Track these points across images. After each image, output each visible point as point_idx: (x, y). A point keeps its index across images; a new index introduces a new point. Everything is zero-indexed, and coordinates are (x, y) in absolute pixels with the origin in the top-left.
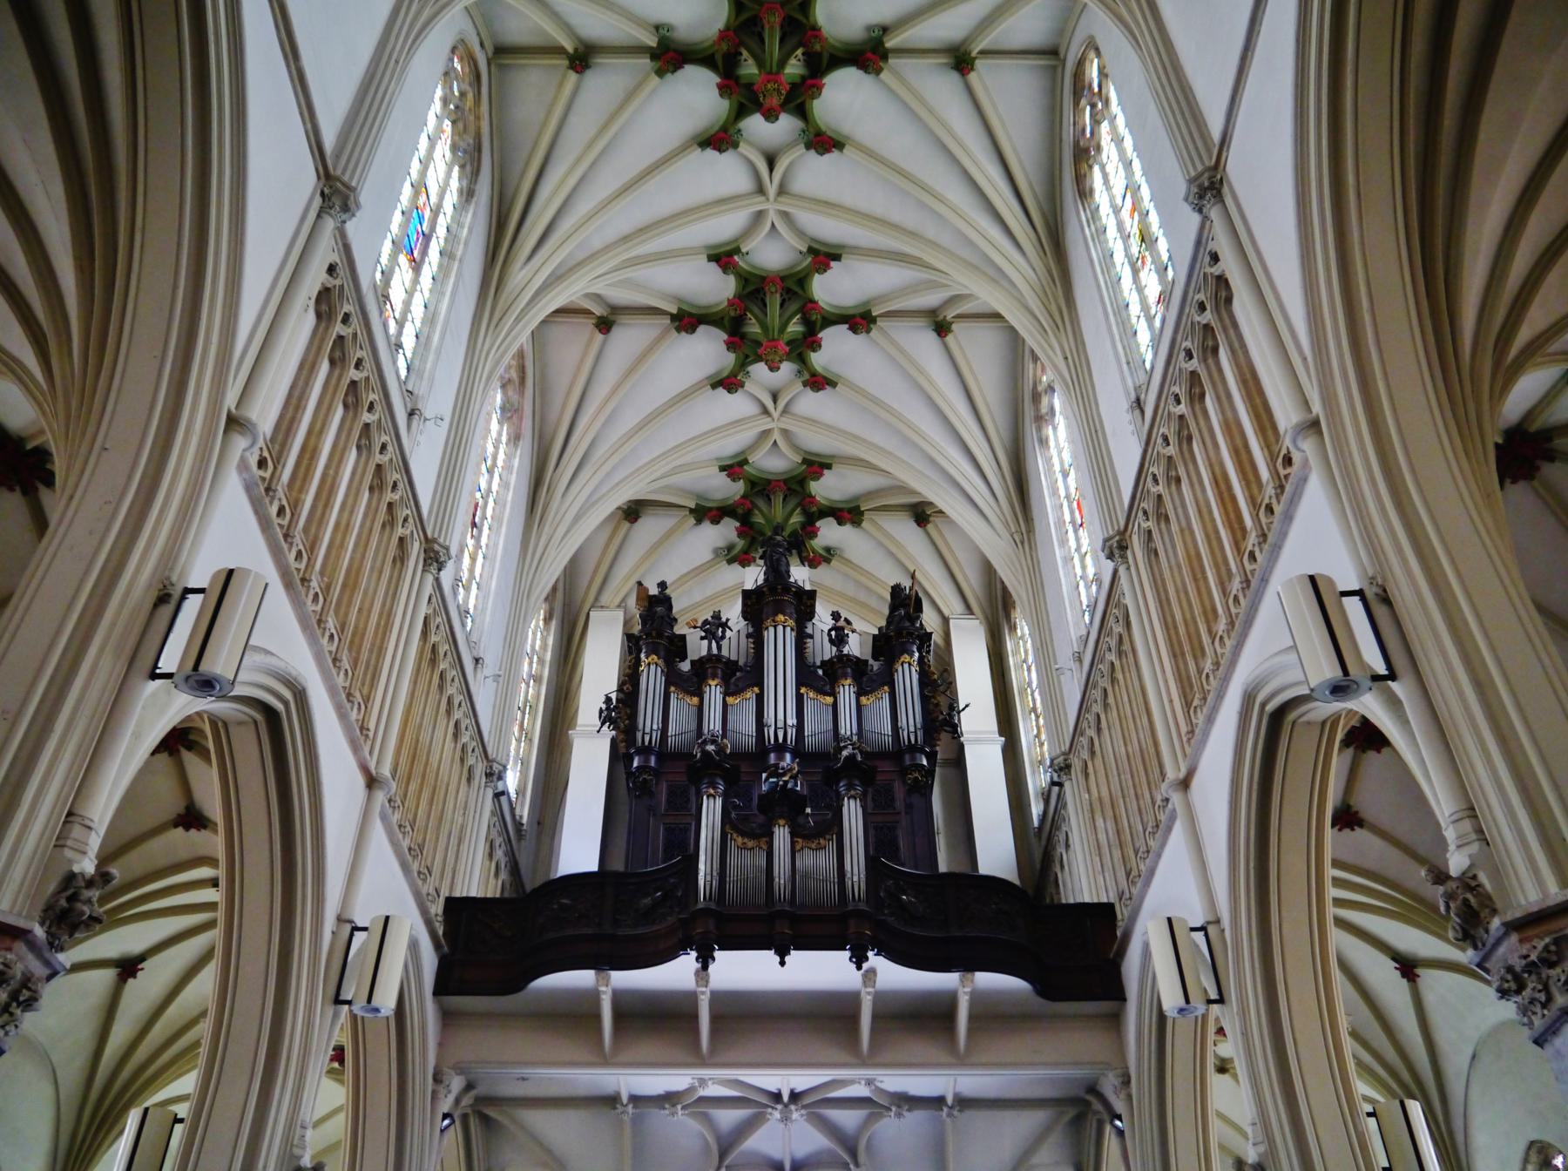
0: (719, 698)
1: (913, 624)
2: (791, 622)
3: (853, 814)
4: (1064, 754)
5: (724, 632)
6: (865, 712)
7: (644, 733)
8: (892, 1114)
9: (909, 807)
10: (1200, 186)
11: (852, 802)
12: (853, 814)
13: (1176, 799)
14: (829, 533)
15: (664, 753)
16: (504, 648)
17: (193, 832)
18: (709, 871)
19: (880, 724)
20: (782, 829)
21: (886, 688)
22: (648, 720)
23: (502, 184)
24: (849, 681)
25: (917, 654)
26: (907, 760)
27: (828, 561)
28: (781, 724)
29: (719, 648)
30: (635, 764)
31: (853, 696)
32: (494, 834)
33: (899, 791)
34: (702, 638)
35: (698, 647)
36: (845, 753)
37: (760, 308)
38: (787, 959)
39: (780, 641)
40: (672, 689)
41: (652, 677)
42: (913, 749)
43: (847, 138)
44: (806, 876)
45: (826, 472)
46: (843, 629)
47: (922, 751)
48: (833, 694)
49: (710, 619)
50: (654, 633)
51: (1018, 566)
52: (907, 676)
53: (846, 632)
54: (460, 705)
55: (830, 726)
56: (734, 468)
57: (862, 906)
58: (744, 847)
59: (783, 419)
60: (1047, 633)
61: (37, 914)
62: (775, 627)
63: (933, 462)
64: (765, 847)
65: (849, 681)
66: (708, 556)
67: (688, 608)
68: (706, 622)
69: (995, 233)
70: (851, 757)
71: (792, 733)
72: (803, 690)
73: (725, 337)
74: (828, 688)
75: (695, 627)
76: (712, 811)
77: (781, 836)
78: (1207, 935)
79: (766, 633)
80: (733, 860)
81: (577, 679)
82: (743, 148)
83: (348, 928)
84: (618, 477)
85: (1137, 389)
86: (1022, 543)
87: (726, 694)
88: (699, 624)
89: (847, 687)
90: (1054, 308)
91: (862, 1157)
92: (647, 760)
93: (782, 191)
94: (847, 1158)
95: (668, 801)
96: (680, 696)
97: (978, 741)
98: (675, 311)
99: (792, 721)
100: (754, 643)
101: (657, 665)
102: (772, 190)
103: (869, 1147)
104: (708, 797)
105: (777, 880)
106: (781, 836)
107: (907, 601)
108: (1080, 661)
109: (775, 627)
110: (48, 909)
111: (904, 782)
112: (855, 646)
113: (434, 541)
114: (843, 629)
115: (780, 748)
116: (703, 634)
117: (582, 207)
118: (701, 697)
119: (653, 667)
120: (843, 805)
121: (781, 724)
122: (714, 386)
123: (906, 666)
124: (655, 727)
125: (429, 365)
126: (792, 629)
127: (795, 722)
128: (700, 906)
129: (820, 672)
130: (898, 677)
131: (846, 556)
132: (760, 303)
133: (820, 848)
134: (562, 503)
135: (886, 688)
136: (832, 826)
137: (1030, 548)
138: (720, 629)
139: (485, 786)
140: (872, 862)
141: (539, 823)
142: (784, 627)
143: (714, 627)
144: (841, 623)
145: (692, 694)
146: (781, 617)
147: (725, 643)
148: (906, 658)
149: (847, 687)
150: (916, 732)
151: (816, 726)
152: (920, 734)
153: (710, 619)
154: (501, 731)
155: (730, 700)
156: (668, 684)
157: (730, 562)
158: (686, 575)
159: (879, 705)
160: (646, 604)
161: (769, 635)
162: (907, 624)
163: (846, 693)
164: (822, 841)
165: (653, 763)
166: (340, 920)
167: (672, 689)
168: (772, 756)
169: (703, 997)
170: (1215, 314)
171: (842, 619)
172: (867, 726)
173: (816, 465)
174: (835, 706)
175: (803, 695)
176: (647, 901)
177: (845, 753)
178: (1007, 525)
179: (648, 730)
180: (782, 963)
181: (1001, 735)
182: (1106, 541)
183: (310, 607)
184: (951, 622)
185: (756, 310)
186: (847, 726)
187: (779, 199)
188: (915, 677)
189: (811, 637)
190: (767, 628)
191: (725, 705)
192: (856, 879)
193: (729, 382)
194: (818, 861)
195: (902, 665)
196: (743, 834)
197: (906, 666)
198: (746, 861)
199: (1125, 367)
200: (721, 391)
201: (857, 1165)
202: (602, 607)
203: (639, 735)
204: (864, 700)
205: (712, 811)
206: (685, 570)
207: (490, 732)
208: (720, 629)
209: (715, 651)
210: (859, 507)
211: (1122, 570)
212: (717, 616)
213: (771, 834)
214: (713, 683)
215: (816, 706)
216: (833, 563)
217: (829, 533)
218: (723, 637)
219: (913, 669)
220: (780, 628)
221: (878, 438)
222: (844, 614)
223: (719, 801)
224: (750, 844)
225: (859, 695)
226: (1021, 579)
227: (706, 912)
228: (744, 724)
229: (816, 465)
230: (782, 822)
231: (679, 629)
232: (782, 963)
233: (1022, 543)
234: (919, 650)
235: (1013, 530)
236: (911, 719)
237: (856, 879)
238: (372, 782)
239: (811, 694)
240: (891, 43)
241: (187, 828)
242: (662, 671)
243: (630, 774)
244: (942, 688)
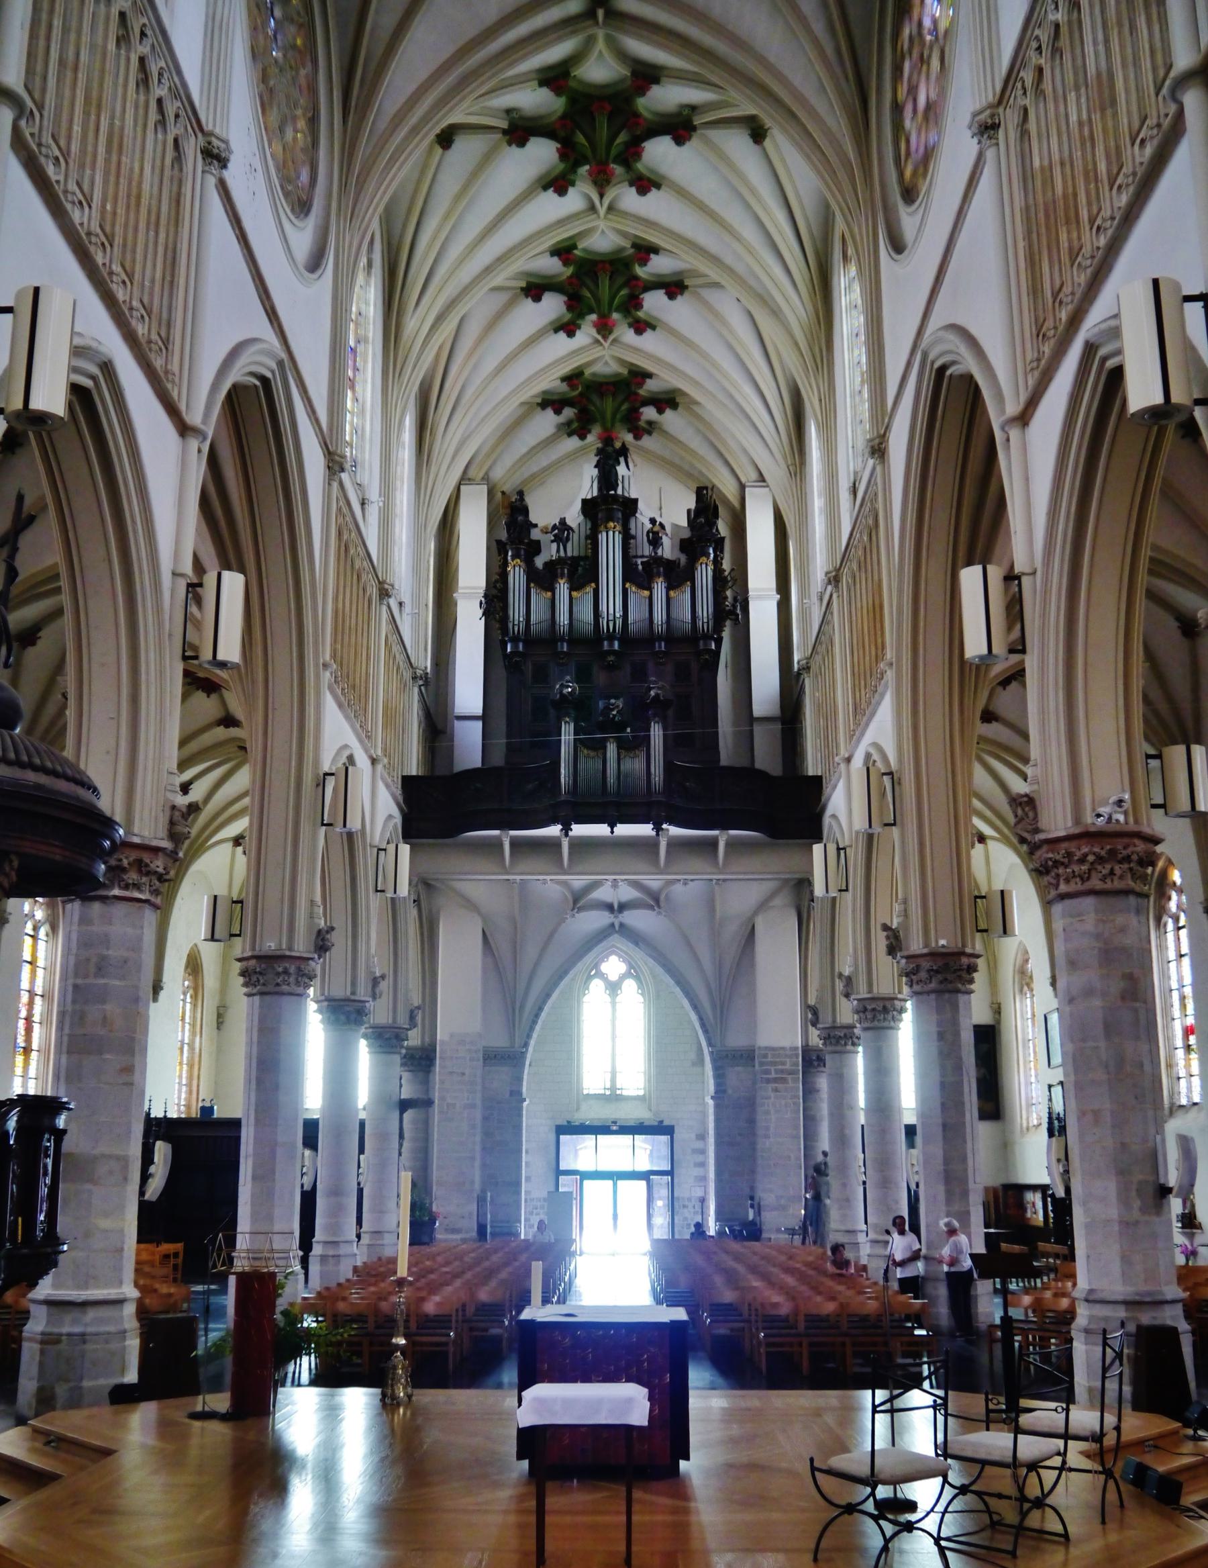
0: (567, 592)
1: (711, 529)
3: (656, 733)
10: (872, 447)
12: (656, 733)
13: (843, 766)
14: (654, 302)
15: (529, 638)
17: (231, 729)
22: (516, 613)
27: (650, 433)
28: (611, 618)
30: (509, 650)
31: (664, 591)
35: (550, 551)
36: (652, 693)
39: (610, 546)
41: (517, 576)
42: (707, 637)
43: (663, 177)
44: (626, 776)
45: (654, 190)
46: (657, 533)
47: (712, 638)
48: (650, 589)
56: (572, 378)
58: (587, 757)
61: (312, 949)
63: (731, 397)
67: (543, 513)
68: (554, 527)
69: (778, 271)
70: (657, 695)
71: (619, 622)
76: (567, 734)
77: (612, 749)
80: (581, 766)
81: (454, 543)
84: (483, 414)
85: (856, 473)
87: (571, 589)
91: (662, 904)
92: (517, 647)
93: (611, 208)
97: (760, 598)
102: (602, 211)
103: (667, 898)
106: (612, 749)
108: (821, 600)
110: (316, 946)
112: (668, 549)
114: (657, 533)
115: (611, 637)
117: (454, 252)
118: (553, 590)
121: (611, 618)
129: (640, 567)
133: (636, 756)
134: (442, 443)
140: (669, 766)
143: (561, 531)
144: (657, 528)
146: (611, 524)
147: (569, 545)
148: (704, 559)
155: (574, 594)
157: (570, 435)
158: (534, 448)
160: (508, 511)
161: (602, 537)
162: (707, 528)
163: (659, 587)
168: (606, 643)
172: (674, 615)
173: (645, 251)
174: (651, 598)
176: (530, 786)
177: (652, 693)
178: (785, 458)
182: (827, 573)
185: (589, 282)
186: (659, 616)
187: (610, 216)
188: (710, 573)
193: (569, 329)
194: (634, 765)
198: (590, 764)
199: (850, 450)
200: (562, 335)
201: (659, 907)
203: (510, 625)
204: (672, 593)
205: (567, 734)
209: (562, 554)
211: (879, 469)
212: (563, 522)
213: (605, 748)
214: (562, 582)
215: (637, 597)
216: (655, 434)
217: (654, 302)
218: (568, 539)
220: (611, 533)
222: (658, 520)
223: (572, 725)
225: (668, 589)
227: (566, 802)
228: (585, 614)
229: (645, 251)
231: (535, 534)
234: (715, 552)
236: (705, 610)
238: (374, 761)
240: (697, 121)
241: (227, 726)
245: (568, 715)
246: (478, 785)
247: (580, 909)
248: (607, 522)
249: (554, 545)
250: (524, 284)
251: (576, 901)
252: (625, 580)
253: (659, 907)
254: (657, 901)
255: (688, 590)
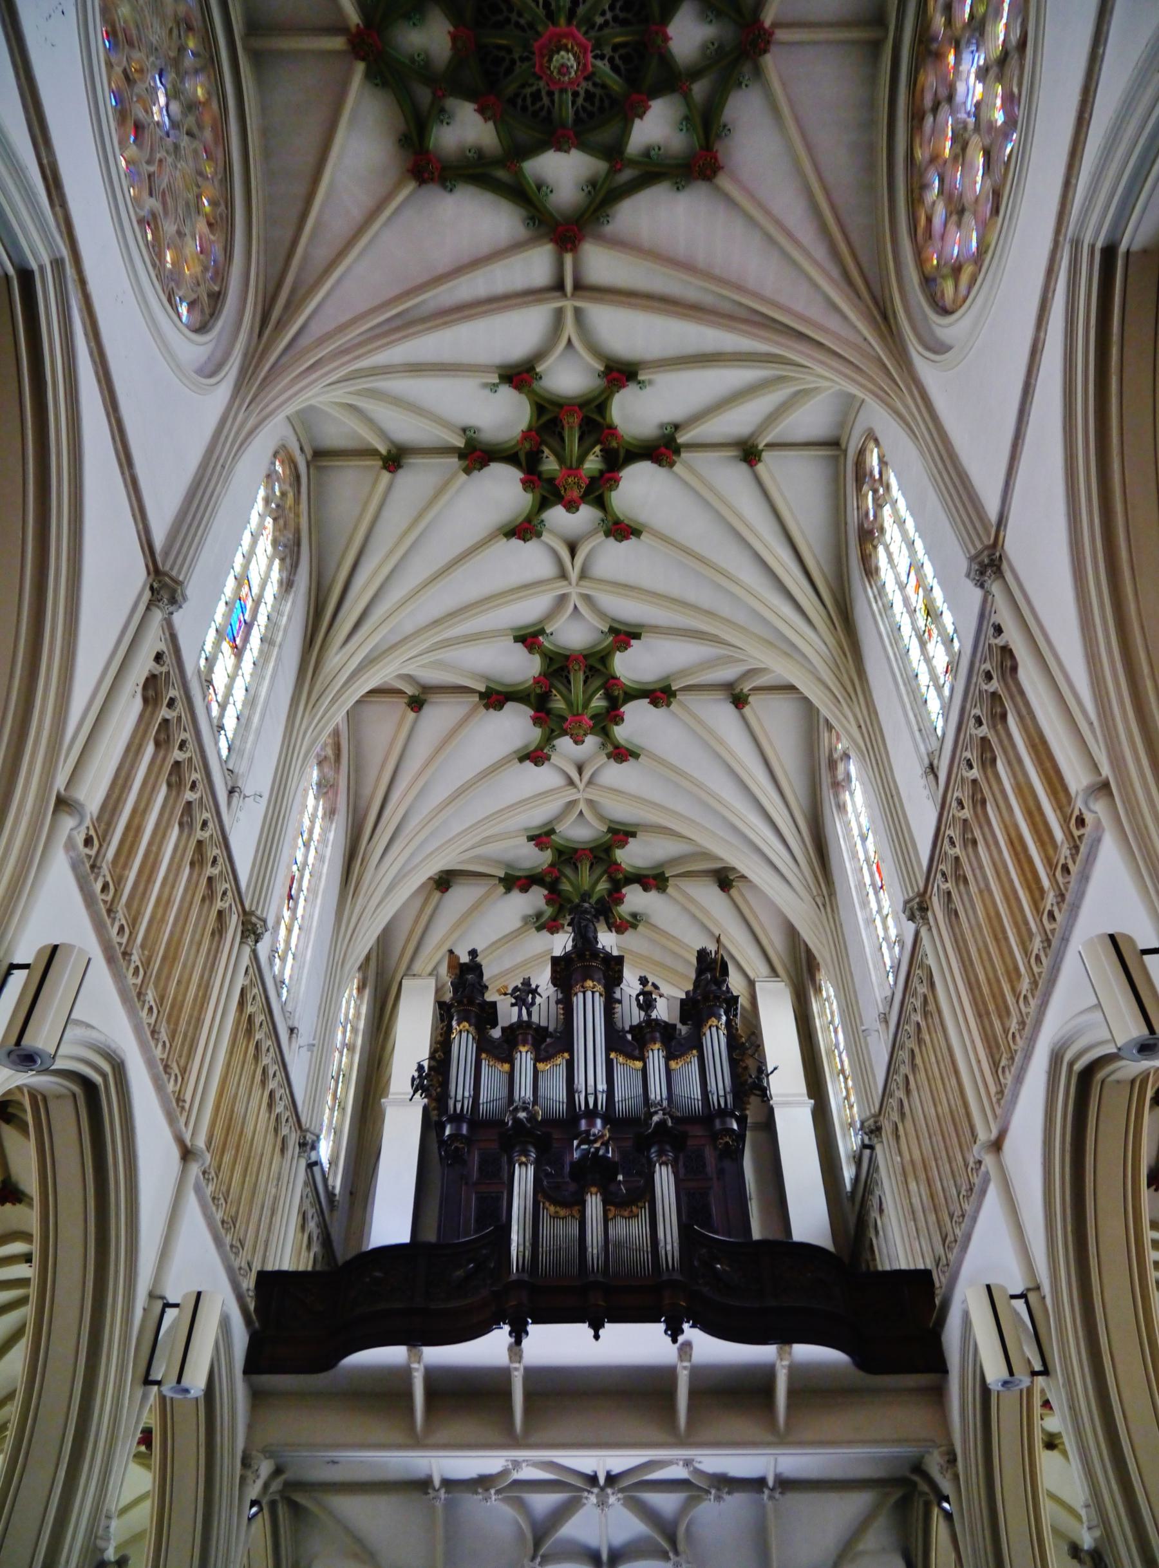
1: (720, 988)
2: (600, 988)
3: (664, 1180)
4: (874, 1116)
5: (534, 998)
6: (675, 1078)
7: (456, 1101)
8: (712, 1497)
9: (721, 1172)
10: (981, 564)
11: (664, 1168)
12: (664, 1180)
13: (989, 1160)
14: (635, 899)
15: (477, 1121)
16: (318, 1017)
18: (521, 1241)
19: (690, 1089)
20: (594, 1197)
21: (695, 1052)
22: (460, 1088)
23: (357, 795)
24: (657, 1046)
25: (724, 1018)
26: (718, 1124)
27: (634, 926)
28: (591, 1090)
29: (529, 1014)
30: (447, 1132)
31: (662, 1061)
32: (307, 1205)
33: (710, 1155)
34: (513, 1005)
35: (509, 1014)
36: (656, 1118)
37: (564, 685)
38: (601, 1332)
40: (484, 1056)
41: (463, 1044)
42: (723, 1113)
43: (644, 525)
44: (619, 1245)
46: (650, 993)
47: (732, 1115)
48: (643, 1059)
49: (520, 986)
50: (465, 1001)
51: (822, 930)
52: (715, 1039)
53: (654, 996)
54: (287, 1120)
55: (641, 1091)
56: (541, 838)
57: (677, 1276)
58: (555, 1217)
59: (588, 790)
60: (852, 993)
62: (584, 993)
64: (577, 1216)
65: (657, 1046)
66: (518, 924)
68: (516, 989)
69: (787, 610)
70: (662, 1123)
71: (602, 1098)
72: (613, 1055)
73: (532, 713)
74: (637, 1053)
75: (505, 994)
76: (524, 1179)
77: (594, 1204)
78: (1027, 1303)
79: (575, 999)
82: (554, 759)
83: (159, 1305)
84: (429, 849)
85: (930, 755)
86: (824, 906)
87: (537, 1060)
88: (510, 991)
89: (656, 1052)
90: (845, 678)
91: (681, 1547)
92: (459, 1128)
93: (583, 575)
94: (666, 1546)
95: (480, 1169)
96: (491, 1063)
98: (483, 690)
99: (602, 1086)
100: (563, 1009)
101: (468, 1032)
102: (574, 575)
104: (520, 1165)
105: (590, 1250)
106: (594, 1204)
107: (713, 965)
108: (886, 1022)
109: (584, 993)
111: (715, 1148)
112: (663, 1011)
113: (252, 913)
114: (650, 993)
115: (591, 1114)
116: (513, 1001)
119: (464, 1035)
120: (654, 1172)
121: (591, 1090)
122: (521, 759)
123: (714, 1029)
124: (467, 1094)
125: (249, 745)
126: (601, 995)
127: (605, 1087)
128: (514, 1277)
129: (629, 1037)
130: (707, 1041)
131: (654, 920)
132: (565, 681)
134: (374, 876)
135: (695, 1052)
136: (645, 1194)
137: (833, 911)
138: (530, 996)
139: (299, 1157)
141: (351, 1193)
142: (593, 993)
143: (524, 994)
144: (649, 988)
145: (503, 1060)
146: (589, 983)
147: (535, 1009)
148: (713, 1021)
149: (656, 1052)
150: (725, 1096)
151: (626, 1091)
152: (730, 1098)
153: (520, 986)
154: (314, 1100)
155: (540, 1066)
156: (479, 1051)
157: (539, 929)
158: (496, 942)
159: (688, 1070)
160: (457, 971)
161: (578, 1001)
162: (714, 988)
163: (656, 1057)
164: (634, 1209)
165: (464, 1130)
166: (152, 1296)
167: (484, 1056)
168: (583, 1122)
169: (516, 1373)
170: (981, 771)
171: (650, 984)
172: (677, 1090)
173: (621, 834)
174: (644, 1071)
175: (612, 1060)
176: (460, 1273)
177: (656, 1118)
178: (808, 889)
179: (459, 1097)
180: (597, 1337)
181: (810, 1096)
182: (906, 903)
183: (171, 1087)
184: (758, 985)
186: (657, 1091)
188: (723, 1040)
189: (620, 1002)
190: (576, 994)
191: (536, 1072)
192: (669, 1248)
193: (536, 756)
195: (710, 1028)
196: (555, 1203)
197: (714, 1029)
199: (917, 734)
200: (528, 764)
201: (677, 1553)
202: (414, 975)
203: (451, 1103)
204: (673, 1064)
205: (524, 1179)
206: (494, 938)
207: (304, 1102)
208: (530, 996)
209: (525, 1017)
210: (663, 873)
211: (924, 932)
212: (527, 982)
213: (582, 1203)
214: (523, 1049)
215: (625, 1070)
216: (641, 928)
217: (635, 899)
218: (533, 1003)
219: (721, 1033)
220: (589, 994)
221: (681, 806)
222: (651, 980)
223: (531, 1170)
224: (562, 1213)
225: (668, 1059)
226: (825, 942)
227: (519, 1284)
229: (621, 834)
230: (594, 1190)
231: (490, 996)
232: (597, 1337)
233: (824, 906)
234: (726, 1013)
235: (815, 893)
236: (720, 1082)
237: (669, 1248)
238: (187, 1154)
239: (621, 1059)
240: (682, 439)
242: (473, 1038)
243: (442, 1143)
244: (750, 1052)
245: (526, 1153)
246: (378, 1274)
247: (545, 1559)
248: (585, 980)
249: (516, 1009)
250: (482, 688)
251: (538, 1543)
252: (608, 1050)
253: (677, 1553)
254: (672, 1540)
255: (695, 1061)
